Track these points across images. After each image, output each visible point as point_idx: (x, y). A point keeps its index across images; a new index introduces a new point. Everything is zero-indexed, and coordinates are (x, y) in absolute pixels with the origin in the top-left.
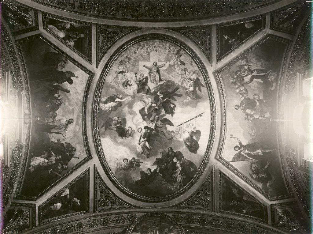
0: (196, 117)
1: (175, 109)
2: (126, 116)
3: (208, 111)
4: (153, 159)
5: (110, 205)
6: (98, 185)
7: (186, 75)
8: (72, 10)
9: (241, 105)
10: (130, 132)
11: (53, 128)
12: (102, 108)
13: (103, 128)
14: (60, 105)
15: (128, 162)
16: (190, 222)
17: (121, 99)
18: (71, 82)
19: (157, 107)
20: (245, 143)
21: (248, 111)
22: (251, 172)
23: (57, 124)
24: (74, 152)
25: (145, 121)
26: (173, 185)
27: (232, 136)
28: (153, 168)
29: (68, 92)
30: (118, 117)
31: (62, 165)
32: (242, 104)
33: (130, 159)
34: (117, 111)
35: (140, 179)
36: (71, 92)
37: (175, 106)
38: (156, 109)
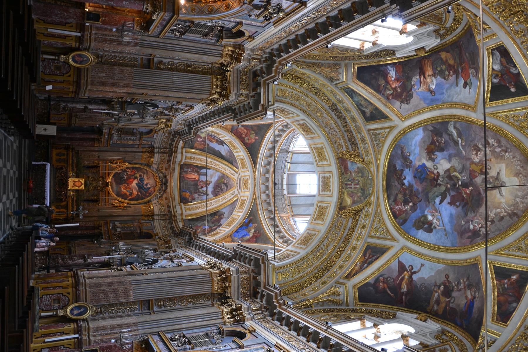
0: (445, 229)
1: (455, 207)
4: (413, 182)
11: (424, 77)
12: (450, 124)
13: (432, 128)
14: (444, 78)
17: (462, 145)
20: (415, 277)
21: (442, 287)
22: (386, 276)
23: (429, 80)
26: (393, 201)
27: (423, 265)
28: (405, 182)
29: (457, 85)
30: (444, 143)
32: (449, 282)
33: (411, 158)
34: (450, 141)
36: (457, 88)
37: (457, 207)
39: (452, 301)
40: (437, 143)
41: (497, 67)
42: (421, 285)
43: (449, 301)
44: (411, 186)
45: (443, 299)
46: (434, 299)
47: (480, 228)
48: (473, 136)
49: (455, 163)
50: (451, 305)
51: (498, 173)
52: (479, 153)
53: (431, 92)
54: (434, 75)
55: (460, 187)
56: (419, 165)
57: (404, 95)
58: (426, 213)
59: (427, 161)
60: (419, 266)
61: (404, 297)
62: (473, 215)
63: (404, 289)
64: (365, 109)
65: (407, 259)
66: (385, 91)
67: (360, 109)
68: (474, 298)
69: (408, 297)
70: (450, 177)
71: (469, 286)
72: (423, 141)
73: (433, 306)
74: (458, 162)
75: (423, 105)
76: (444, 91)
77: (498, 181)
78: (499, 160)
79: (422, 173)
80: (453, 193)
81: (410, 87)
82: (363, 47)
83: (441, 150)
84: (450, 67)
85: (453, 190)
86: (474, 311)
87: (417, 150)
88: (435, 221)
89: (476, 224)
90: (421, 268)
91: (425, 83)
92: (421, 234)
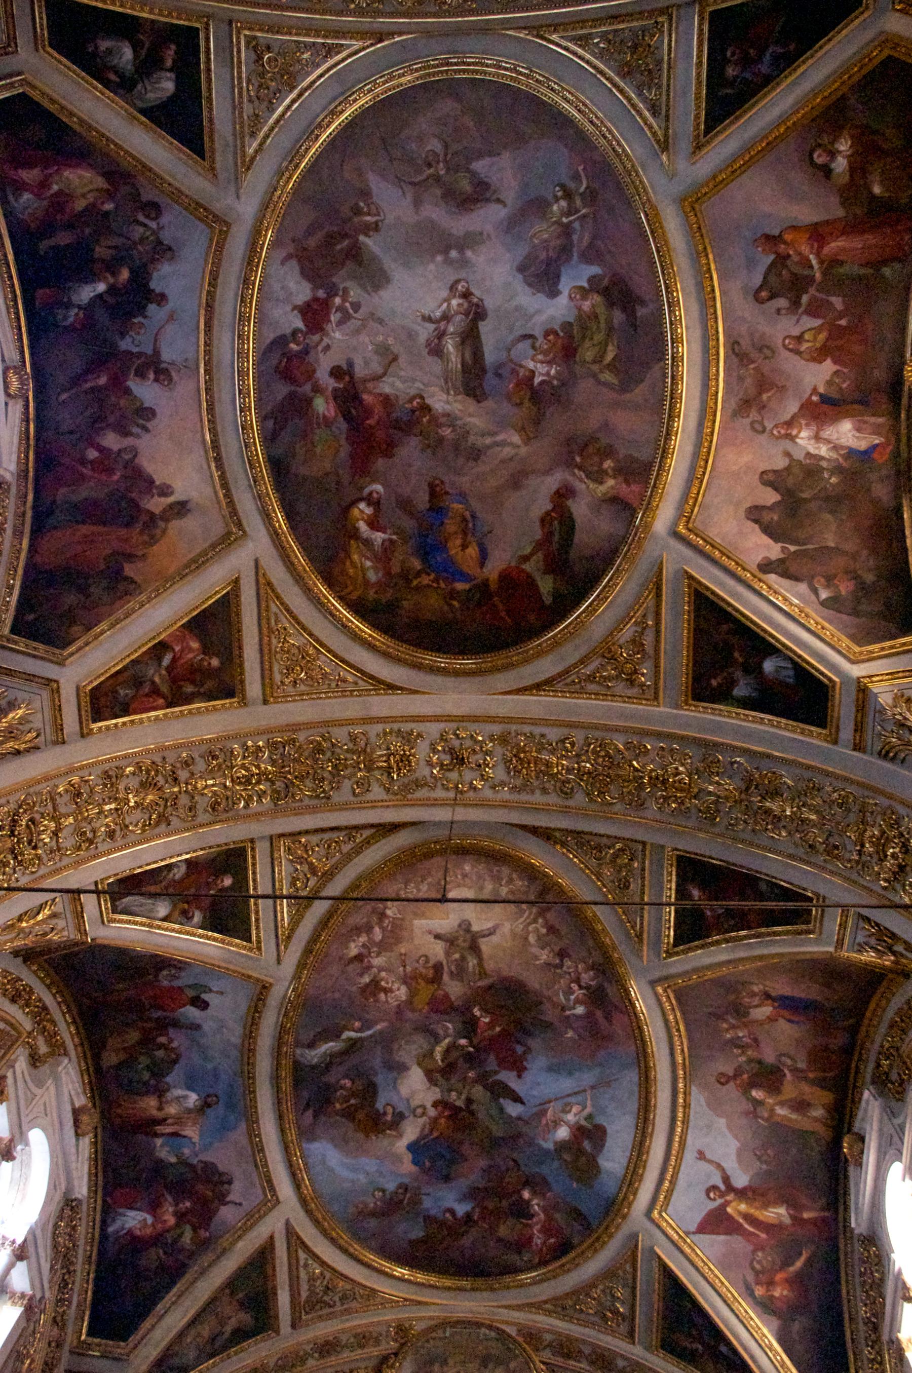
0: (593, 1088)
1: (529, 1057)
2: (376, 1074)
3: (631, 1077)
5: (338, 1304)
6: (302, 1263)
7: (565, 968)
8: (188, 824)
9: (735, 1077)
10: (389, 1118)
12: (302, 1059)
13: (310, 1113)
14: (175, 1062)
15: (388, 1196)
16: (568, 1356)
17: (359, 1030)
18: (204, 1006)
19: (471, 1049)
20: (741, 1180)
21: (757, 1094)
22: (750, 1278)
23: (172, 1110)
24: (226, 1186)
25: (436, 1085)
27: (701, 1156)
28: (461, 1209)
29: (198, 1027)
31: (195, 1229)
32: (737, 1074)
33: (391, 1186)
35: (422, 1234)
37: (528, 1050)
38: (469, 1053)
39: (789, 1062)
40: (353, 1101)
41: (163, 909)
42: (759, 1158)
43: (790, 1071)
44: (473, 1194)
45: (790, 1088)
46: (794, 1116)
47: (581, 987)
48: (337, 995)
49: (409, 1051)
50: (801, 1065)
51: (437, 937)
52: (383, 983)
53: (206, 1105)
54: (160, 1092)
55: (475, 1041)
56: (415, 1162)
57: (201, 1190)
58: (549, 1145)
59: (400, 1136)
60: (703, 1165)
61: (806, 1215)
62: (547, 1006)
63: (778, 1213)
64: (228, 1329)
65: (688, 1205)
66: (181, 1250)
67: (225, 1348)
68: (768, 996)
69: (804, 1201)
70: (449, 1069)
71: (740, 1011)
72: (342, 1143)
73: (816, 1119)
74: (407, 1042)
75: (239, 1135)
76: (210, 1066)
77: (457, 938)
78: (405, 934)
79: (436, 1156)
80: (492, 1062)
81: (183, 1170)
82: (23, 1296)
83: (370, 1091)
84: (147, 1041)
85: (481, 1063)
86: (803, 995)
87: (369, 1164)
88: (570, 1117)
89: (572, 997)
90: (710, 1162)
91: (179, 1120)
92: (613, 1160)
